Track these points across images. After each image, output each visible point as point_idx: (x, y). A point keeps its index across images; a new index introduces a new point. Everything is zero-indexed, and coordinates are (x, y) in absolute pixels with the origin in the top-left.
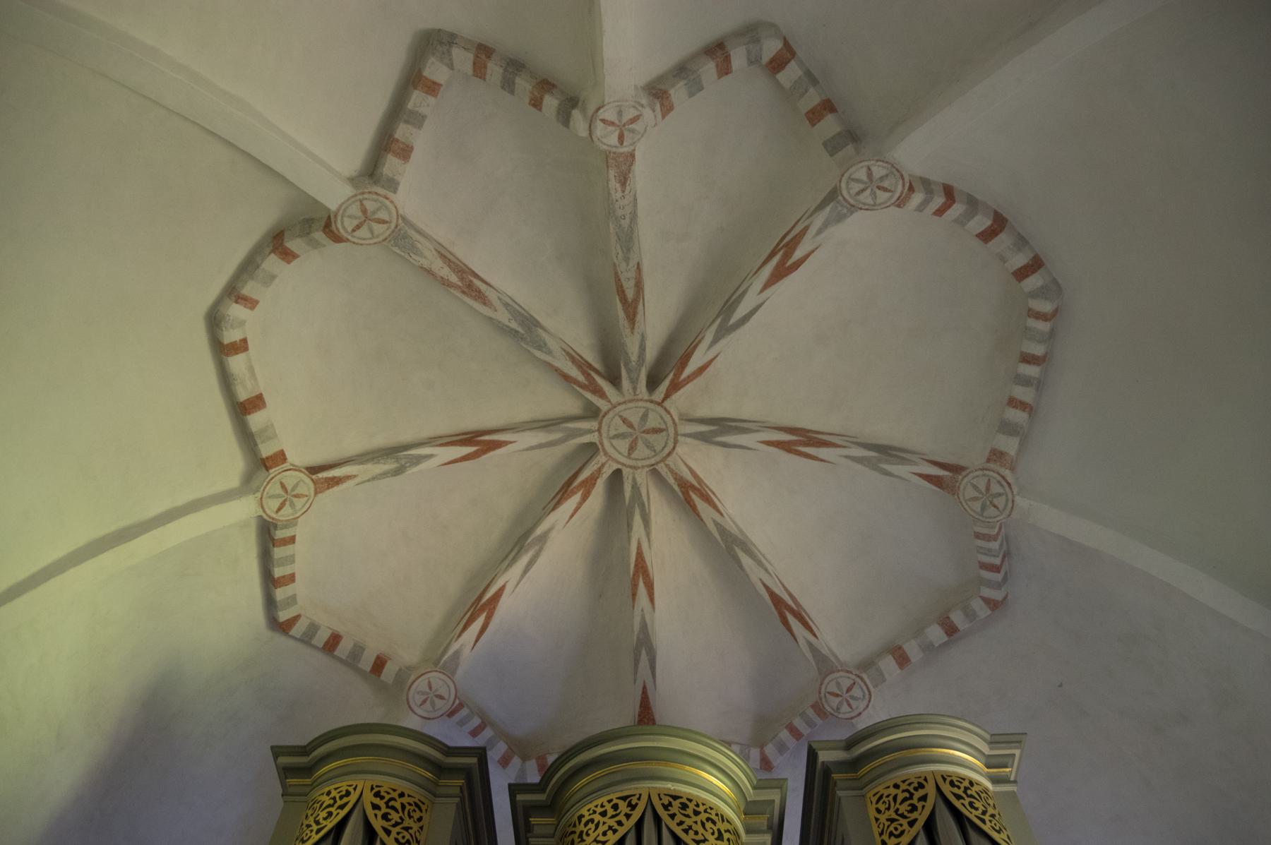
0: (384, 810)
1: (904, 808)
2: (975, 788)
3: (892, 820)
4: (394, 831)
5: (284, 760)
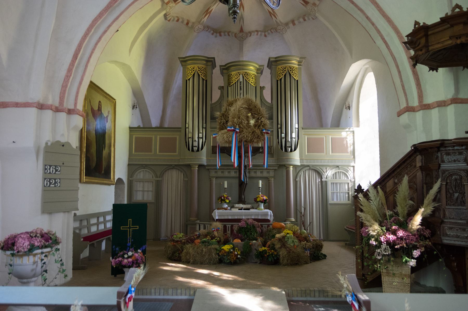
0: (200, 71)
1: (282, 72)
2: (295, 68)
3: (280, 73)
4: (202, 74)
5: (181, 60)
